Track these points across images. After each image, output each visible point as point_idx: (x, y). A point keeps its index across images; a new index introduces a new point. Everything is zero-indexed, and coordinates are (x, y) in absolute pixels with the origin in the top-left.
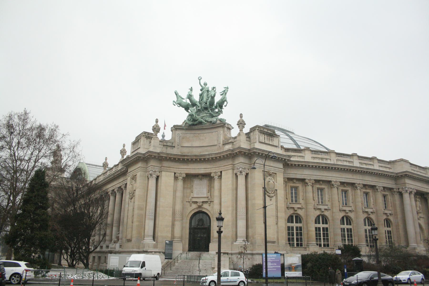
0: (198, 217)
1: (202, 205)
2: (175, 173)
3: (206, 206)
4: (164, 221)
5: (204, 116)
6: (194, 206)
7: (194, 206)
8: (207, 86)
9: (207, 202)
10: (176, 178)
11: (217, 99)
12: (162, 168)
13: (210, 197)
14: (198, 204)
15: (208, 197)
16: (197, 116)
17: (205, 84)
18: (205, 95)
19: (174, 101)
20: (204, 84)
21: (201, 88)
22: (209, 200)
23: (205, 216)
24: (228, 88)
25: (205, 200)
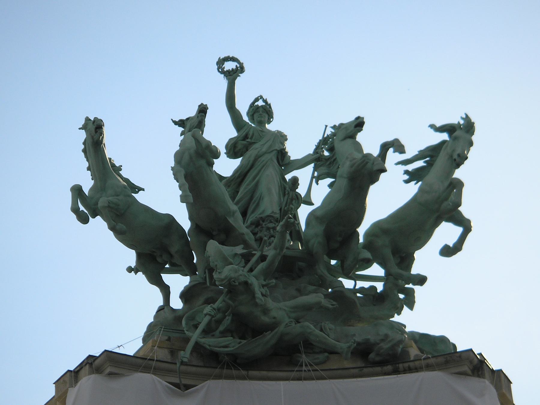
5: (308, 308)
8: (271, 127)
11: (388, 197)
16: (270, 303)
17: (262, 112)
18: (268, 180)
19: (77, 191)
20: (254, 110)
21: (234, 133)
24: (468, 127)
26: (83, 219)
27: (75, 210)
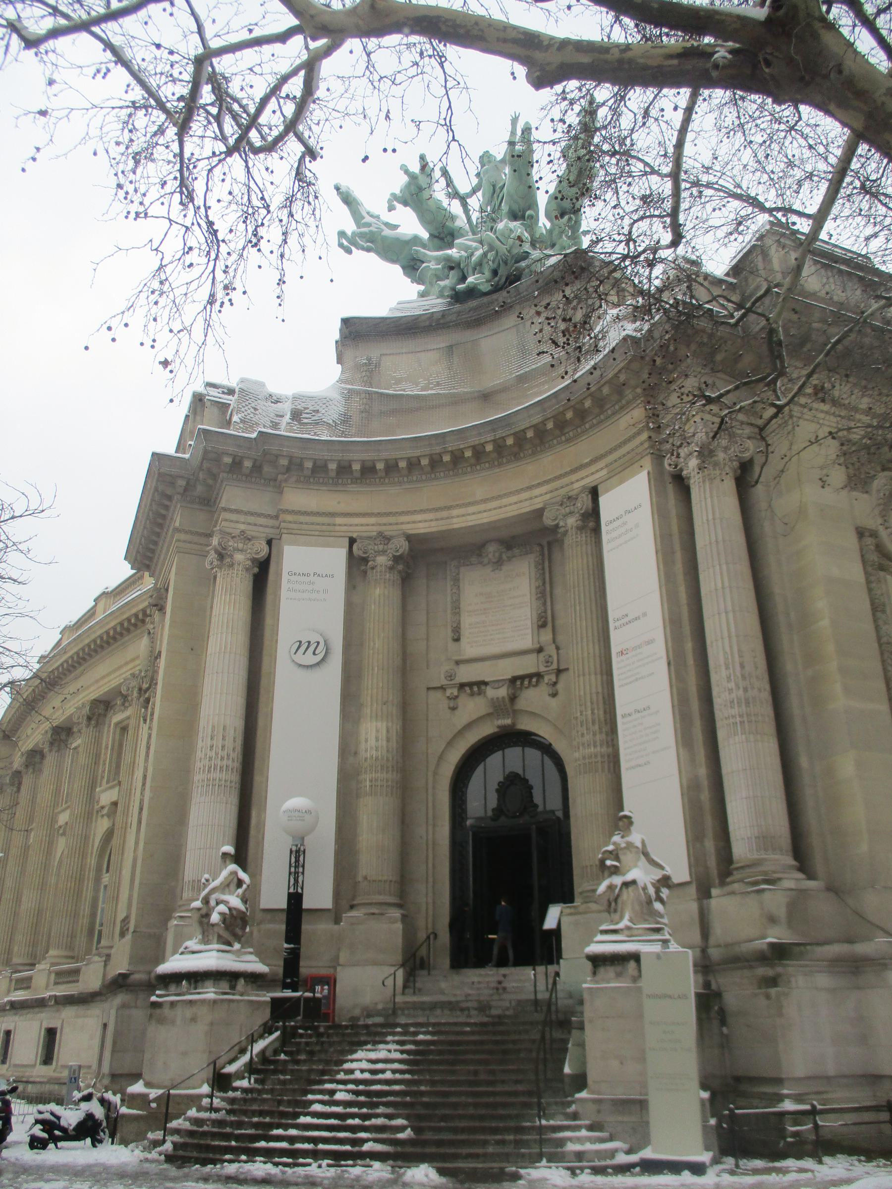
0: (495, 767)
1: (513, 698)
2: (352, 541)
3: (533, 698)
4: (300, 793)
6: (472, 707)
7: (472, 707)
9: (539, 676)
10: (358, 565)
12: (283, 516)
13: (551, 650)
14: (490, 692)
15: (540, 650)
19: (342, 234)
22: (548, 662)
23: (533, 754)
25: (528, 665)
26: (349, 252)
27: (341, 245)
